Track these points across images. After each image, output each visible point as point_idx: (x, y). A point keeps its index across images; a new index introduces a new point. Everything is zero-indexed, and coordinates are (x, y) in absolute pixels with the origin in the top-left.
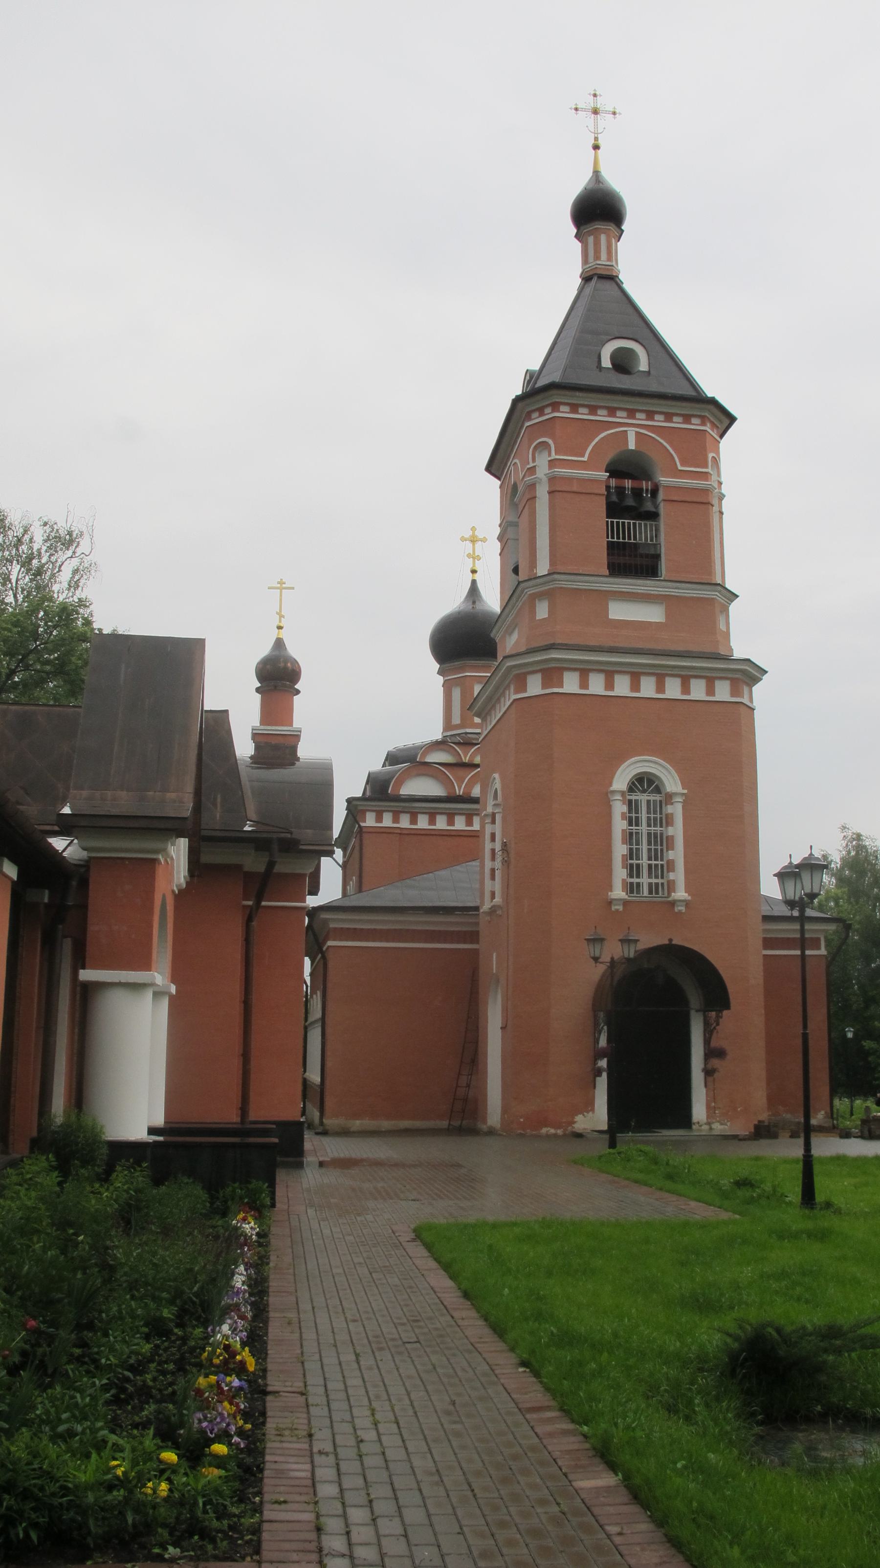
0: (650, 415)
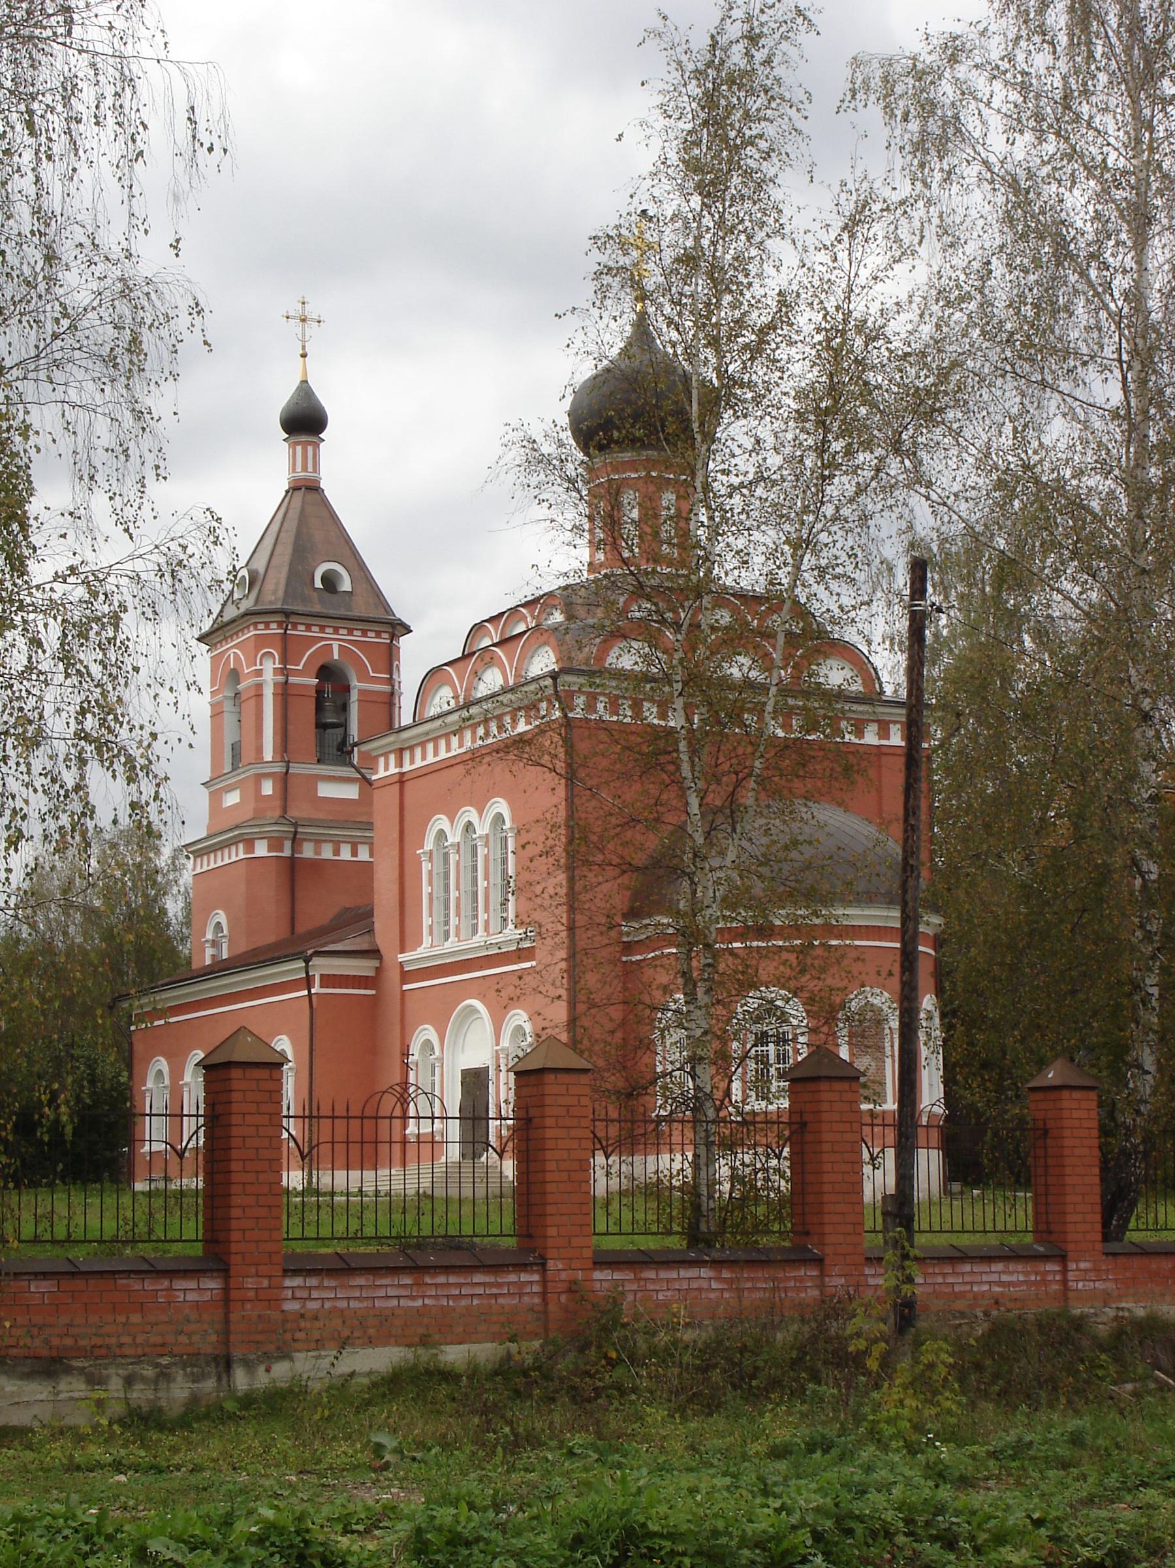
0: (350, 632)
